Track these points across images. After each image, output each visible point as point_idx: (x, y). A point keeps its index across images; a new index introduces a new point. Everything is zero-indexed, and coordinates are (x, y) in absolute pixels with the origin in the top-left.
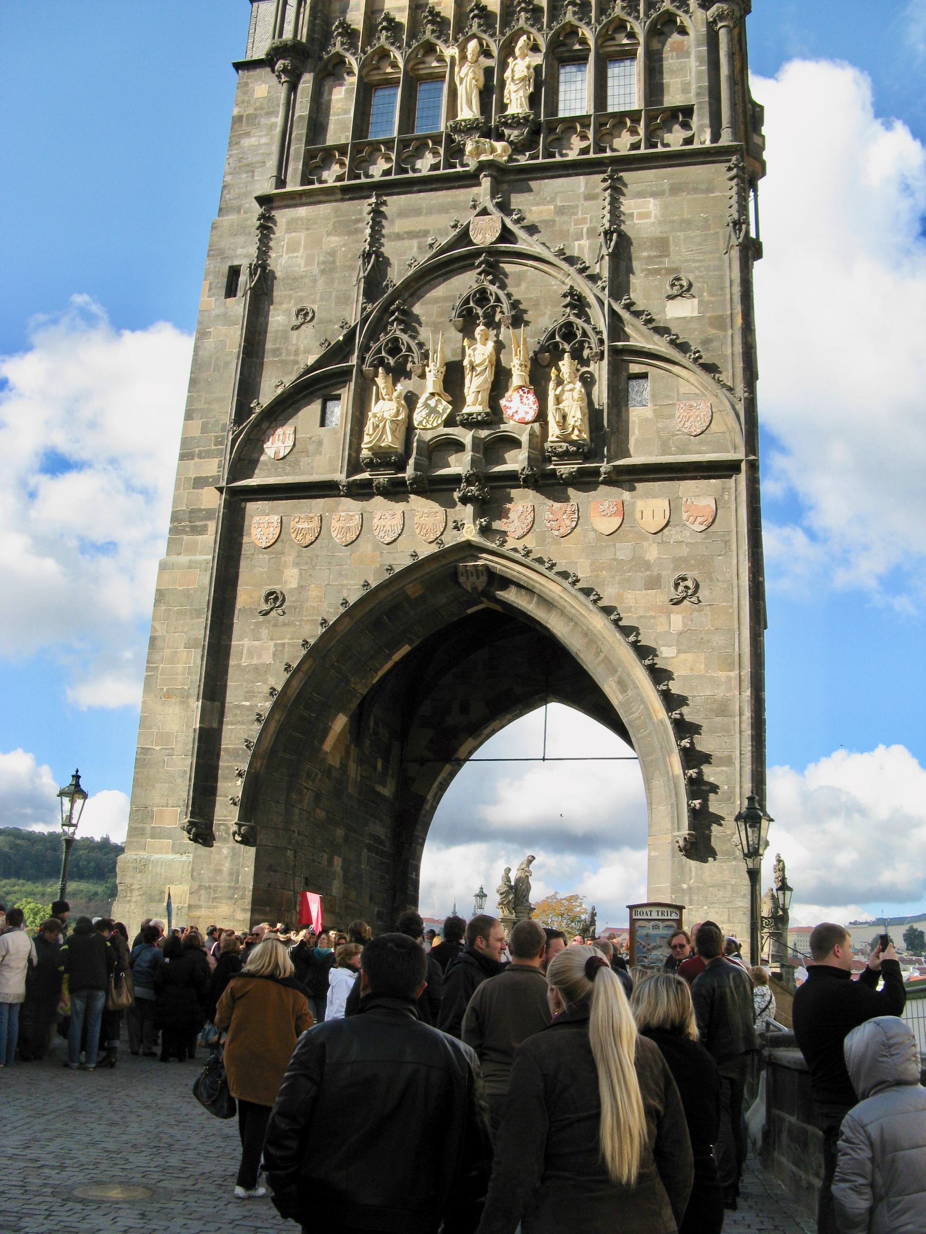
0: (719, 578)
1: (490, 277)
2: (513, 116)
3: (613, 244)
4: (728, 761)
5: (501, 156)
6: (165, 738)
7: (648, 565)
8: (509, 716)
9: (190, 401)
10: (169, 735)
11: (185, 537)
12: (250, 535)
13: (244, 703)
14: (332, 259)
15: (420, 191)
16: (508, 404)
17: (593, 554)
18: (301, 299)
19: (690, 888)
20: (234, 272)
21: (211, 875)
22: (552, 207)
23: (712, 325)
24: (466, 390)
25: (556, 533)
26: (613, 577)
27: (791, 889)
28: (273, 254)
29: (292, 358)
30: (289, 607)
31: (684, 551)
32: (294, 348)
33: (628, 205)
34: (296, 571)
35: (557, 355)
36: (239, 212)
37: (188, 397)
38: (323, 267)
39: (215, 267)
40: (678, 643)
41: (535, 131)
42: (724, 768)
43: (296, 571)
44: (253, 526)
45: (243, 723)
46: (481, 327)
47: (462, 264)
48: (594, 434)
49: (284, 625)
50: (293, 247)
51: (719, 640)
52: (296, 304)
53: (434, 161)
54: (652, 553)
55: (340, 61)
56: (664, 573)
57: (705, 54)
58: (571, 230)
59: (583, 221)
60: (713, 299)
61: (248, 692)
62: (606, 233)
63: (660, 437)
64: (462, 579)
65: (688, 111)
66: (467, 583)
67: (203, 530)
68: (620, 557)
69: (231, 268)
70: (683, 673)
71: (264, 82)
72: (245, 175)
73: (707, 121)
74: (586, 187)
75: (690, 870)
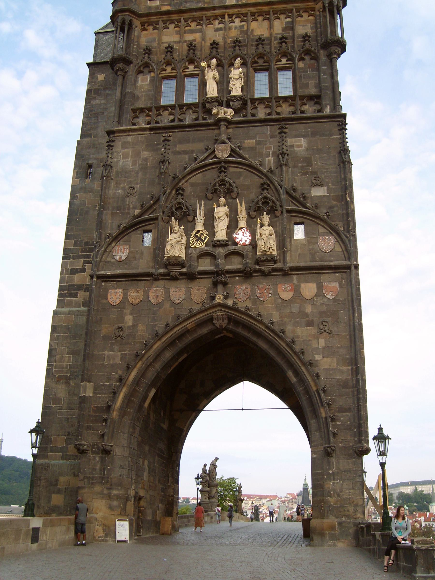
0: (342, 321)
2: (235, 96)
4: (349, 410)
6: (57, 401)
7: (307, 315)
8: (224, 388)
9: (67, 230)
10: (59, 399)
11: (66, 299)
12: (107, 299)
13: (106, 383)
14: (145, 163)
15: (189, 131)
16: (237, 236)
17: (280, 309)
18: (131, 182)
19: (333, 473)
21: (90, 471)
22: (254, 141)
23: (334, 200)
26: (290, 321)
29: (126, 211)
30: (127, 335)
31: (324, 308)
32: (127, 206)
33: (290, 141)
34: (131, 317)
36: (91, 137)
37: (67, 228)
38: (141, 166)
41: (245, 104)
42: (348, 414)
43: (131, 317)
44: (109, 294)
45: (105, 394)
46: (222, 198)
47: (211, 167)
48: (279, 251)
49: (126, 344)
50: (125, 156)
51: (343, 351)
52: (128, 185)
54: (309, 309)
55: (147, 65)
60: (334, 187)
61: (107, 378)
62: (281, 154)
63: (310, 253)
64: (215, 322)
67: (76, 295)
69: (88, 164)
70: (326, 367)
71: (103, 73)
74: (271, 131)
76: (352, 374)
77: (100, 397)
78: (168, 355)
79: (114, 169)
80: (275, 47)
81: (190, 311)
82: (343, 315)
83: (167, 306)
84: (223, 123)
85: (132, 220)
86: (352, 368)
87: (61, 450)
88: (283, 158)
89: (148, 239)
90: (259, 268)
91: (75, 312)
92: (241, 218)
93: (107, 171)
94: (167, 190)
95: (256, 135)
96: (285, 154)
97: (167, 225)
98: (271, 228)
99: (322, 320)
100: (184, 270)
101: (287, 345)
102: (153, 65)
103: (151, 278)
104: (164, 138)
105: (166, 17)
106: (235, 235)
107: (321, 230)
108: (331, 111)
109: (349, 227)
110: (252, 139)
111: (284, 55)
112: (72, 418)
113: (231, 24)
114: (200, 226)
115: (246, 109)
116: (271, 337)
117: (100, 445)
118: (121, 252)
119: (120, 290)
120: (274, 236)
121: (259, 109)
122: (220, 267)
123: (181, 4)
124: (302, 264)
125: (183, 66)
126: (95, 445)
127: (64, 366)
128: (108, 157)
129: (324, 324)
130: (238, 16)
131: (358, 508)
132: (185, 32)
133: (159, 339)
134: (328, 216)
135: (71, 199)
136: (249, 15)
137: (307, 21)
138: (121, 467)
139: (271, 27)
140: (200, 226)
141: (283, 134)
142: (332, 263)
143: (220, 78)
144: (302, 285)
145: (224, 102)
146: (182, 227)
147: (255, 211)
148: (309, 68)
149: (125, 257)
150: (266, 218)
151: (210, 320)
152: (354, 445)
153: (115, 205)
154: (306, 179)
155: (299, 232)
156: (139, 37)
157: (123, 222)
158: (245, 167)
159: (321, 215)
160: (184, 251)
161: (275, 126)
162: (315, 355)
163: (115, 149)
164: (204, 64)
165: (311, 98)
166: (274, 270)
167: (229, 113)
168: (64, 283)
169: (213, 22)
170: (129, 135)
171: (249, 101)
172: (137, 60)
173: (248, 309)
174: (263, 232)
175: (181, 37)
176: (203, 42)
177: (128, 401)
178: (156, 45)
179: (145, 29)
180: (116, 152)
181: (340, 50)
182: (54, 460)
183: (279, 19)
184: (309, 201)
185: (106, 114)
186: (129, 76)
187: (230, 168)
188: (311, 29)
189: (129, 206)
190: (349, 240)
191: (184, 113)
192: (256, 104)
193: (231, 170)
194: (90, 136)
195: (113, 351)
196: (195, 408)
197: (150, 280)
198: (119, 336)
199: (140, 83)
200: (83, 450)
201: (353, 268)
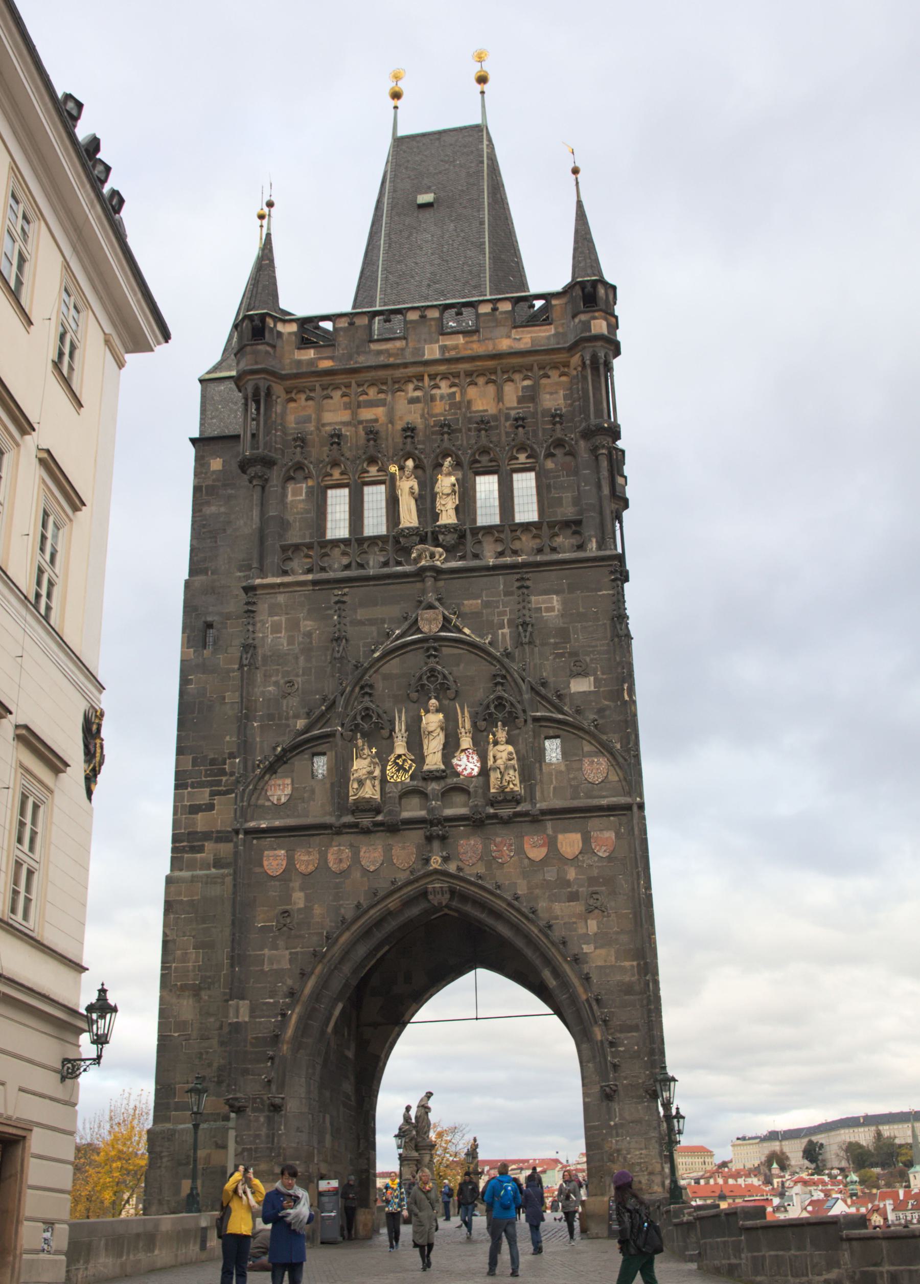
1: (437, 659)
2: (445, 526)
3: (528, 634)
4: (635, 1028)
6: (181, 1025)
7: (568, 883)
8: (444, 983)
10: (185, 1023)
11: (186, 855)
12: (262, 866)
15: (374, 585)
16: (459, 763)
19: (615, 1125)
23: (605, 699)
27: (683, 1118)
31: (595, 872)
35: (491, 721)
36: (207, 574)
41: (462, 536)
42: (634, 1034)
45: (268, 1017)
46: (433, 701)
47: (413, 647)
50: (276, 629)
51: (624, 938)
52: (283, 677)
53: (382, 559)
54: (571, 874)
55: (299, 467)
56: (581, 890)
58: (495, 621)
59: (504, 613)
60: (605, 677)
61: (271, 992)
62: (522, 625)
63: (571, 786)
64: (431, 897)
65: (578, 523)
66: (435, 900)
67: (201, 849)
69: (205, 622)
70: (599, 964)
72: (209, 541)
73: (593, 533)
76: (639, 973)
77: (260, 1023)
78: (362, 951)
79: (260, 651)
80: (507, 433)
81: (393, 883)
82: (623, 884)
83: (356, 875)
84: (428, 574)
85: (294, 739)
86: (638, 965)
88: (525, 631)
89: (321, 765)
92: (463, 734)
93: (249, 656)
94: (346, 687)
95: (482, 590)
96: (528, 624)
97: (349, 744)
98: (510, 748)
100: (380, 818)
101: (540, 931)
102: (311, 466)
103: (330, 831)
104: (337, 599)
105: (326, 380)
106: (455, 761)
107: (587, 748)
108: (599, 548)
109: (629, 743)
110: (477, 598)
111: (522, 448)
112: (207, 1053)
113: (434, 391)
114: (400, 748)
115: (464, 544)
117: (265, 1097)
118: (280, 790)
119: (283, 852)
120: (514, 762)
121: (485, 544)
122: (436, 812)
123: (350, 357)
124: (558, 803)
125: (360, 468)
127: (191, 968)
128: (248, 630)
129: (595, 896)
130: (445, 377)
131: (653, 1178)
132: (359, 406)
133: (348, 929)
134: (596, 726)
135: (181, 685)
136: (462, 373)
137: (557, 384)
138: (298, 1130)
139: (500, 397)
140: (400, 748)
141: (525, 591)
142: (604, 802)
143: (420, 490)
144: (560, 837)
145: (429, 534)
146: (374, 750)
147: (485, 720)
149: (287, 798)
151: (424, 894)
152: (644, 1082)
155: (553, 750)
156: (284, 414)
157: (280, 739)
159: (585, 724)
160: (378, 788)
161: (511, 576)
164: (393, 469)
165: (566, 524)
166: (517, 815)
167: (440, 558)
168: (180, 829)
169: (404, 388)
170: (280, 593)
171: (468, 532)
172: (283, 456)
173: (480, 877)
174: (499, 755)
175: (354, 414)
176: (390, 426)
177: (303, 1027)
178: (312, 429)
179: (292, 400)
180: (260, 621)
181: (610, 440)
183: (512, 381)
184: (567, 700)
185: (229, 531)
186: (273, 486)
187: (444, 649)
188: (564, 399)
189: (288, 713)
190: (629, 764)
191: (366, 552)
192: (480, 536)
193: (446, 651)
194: (204, 571)
195: (277, 949)
196: (396, 1019)
199: (290, 498)
200: (239, 1108)
201: (635, 808)
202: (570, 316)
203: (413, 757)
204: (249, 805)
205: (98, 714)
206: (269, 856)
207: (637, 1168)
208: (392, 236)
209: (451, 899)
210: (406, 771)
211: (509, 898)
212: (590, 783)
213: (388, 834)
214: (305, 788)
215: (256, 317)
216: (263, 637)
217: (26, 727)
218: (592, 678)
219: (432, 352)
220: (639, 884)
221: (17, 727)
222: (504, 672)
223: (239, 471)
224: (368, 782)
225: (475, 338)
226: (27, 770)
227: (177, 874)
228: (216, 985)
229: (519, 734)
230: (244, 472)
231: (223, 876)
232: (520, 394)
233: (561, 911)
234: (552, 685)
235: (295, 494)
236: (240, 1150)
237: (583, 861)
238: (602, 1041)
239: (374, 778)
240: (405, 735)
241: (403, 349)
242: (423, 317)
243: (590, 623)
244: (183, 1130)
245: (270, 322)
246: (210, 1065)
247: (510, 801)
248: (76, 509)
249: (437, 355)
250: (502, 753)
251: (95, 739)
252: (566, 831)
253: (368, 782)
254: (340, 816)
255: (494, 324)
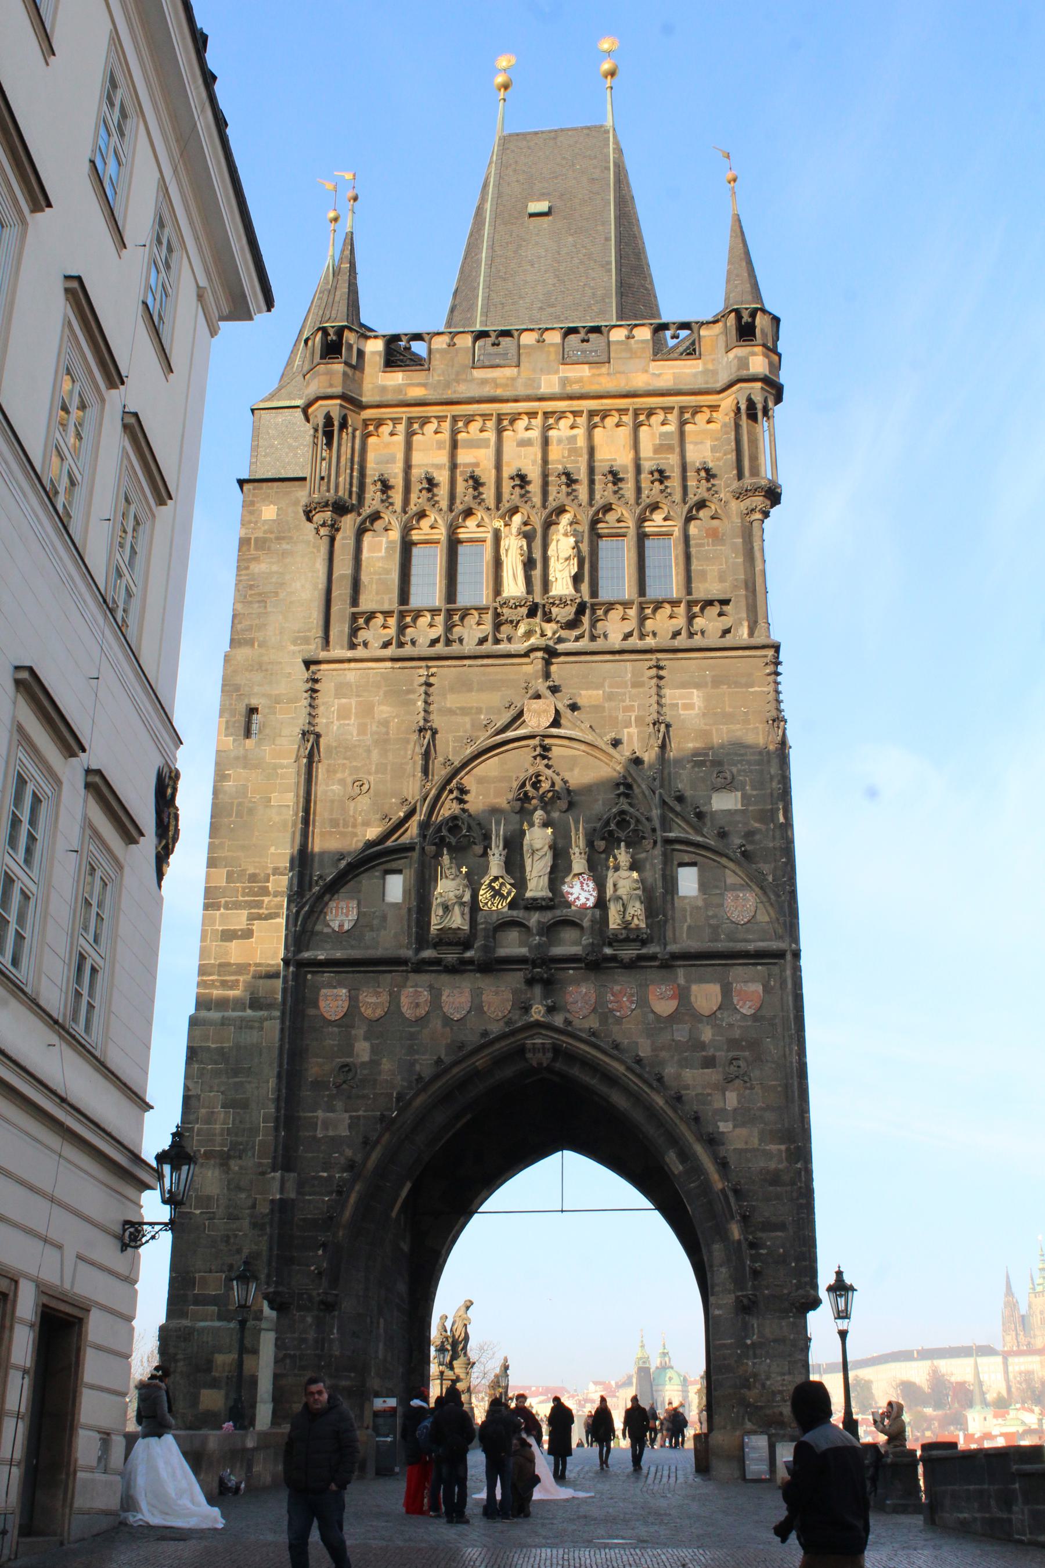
0: (769, 1058)
1: (546, 761)
4: (782, 1227)
5: (550, 639)
7: (702, 1046)
9: (212, 848)
10: (209, 1198)
12: (316, 1006)
13: (321, 1174)
14: (384, 730)
18: (356, 769)
19: (753, 1344)
20: (253, 711)
24: (528, 873)
25: (618, 1014)
28: (321, 721)
29: (350, 829)
31: (737, 1034)
35: (612, 841)
36: (253, 645)
38: (376, 737)
39: (231, 704)
40: (734, 1120)
42: (779, 1234)
44: (321, 998)
50: (344, 714)
51: (770, 1116)
52: (351, 774)
54: (707, 1034)
56: (718, 1054)
57: (741, 546)
60: (755, 793)
62: (654, 724)
63: (710, 926)
64: (529, 1055)
65: (725, 602)
66: (534, 1059)
68: (678, 1037)
70: (740, 1145)
71: (271, 503)
72: (257, 605)
73: (744, 615)
74: (633, 675)
75: (753, 1325)
83: (437, 1024)
86: (788, 1150)
87: (214, 1300)
89: (395, 888)
90: (614, 955)
91: (234, 1019)
94: (431, 789)
95: (604, 679)
97: (433, 861)
98: (635, 875)
99: (731, 1054)
100: (469, 954)
105: (416, 411)
106: (565, 888)
107: (731, 879)
108: (751, 634)
110: (597, 688)
112: (236, 1236)
116: (636, 1088)
117: (314, 1293)
119: (344, 991)
120: (639, 892)
123: (447, 385)
126: (302, 1294)
127: (217, 1131)
133: (424, 1089)
134: (744, 854)
137: (705, 432)
142: (751, 947)
144: (694, 988)
146: (464, 870)
147: (603, 839)
148: (707, 536)
150: (623, 856)
151: (521, 1051)
152: (790, 1293)
153: (326, 815)
154: (702, 775)
158: (583, 747)
160: (467, 917)
162: (719, 1123)
163: (321, 699)
165: (710, 603)
166: (641, 958)
168: (210, 959)
173: (594, 1034)
174: (621, 883)
178: (396, 471)
180: (323, 704)
182: (202, 1320)
185: (282, 595)
189: (356, 820)
194: (250, 643)
195: (333, 1111)
197: (403, 971)
198: (344, 1082)
199: (365, 554)
201: (789, 957)
202: (723, 350)
203: (512, 881)
204: (304, 930)
205: (173, 775)
206: (326, 996)
207: (778, 1398)
208: (497, 248)
209: (554, 1059)
210: (504, 898)
211: (629, 1061)
212: (733, 922)
213: (478, 975)
214: (374, 913)
215: (331, 331)
216: (327, 725)
217: (99, 772)
218: (739, 794)
219: (549, 384)
220: (791, 1050)
221: (88, 771)
222: (630, 780)
223: (304, 518)
224: (456, 908)
225: (604, 369)
226: (96, 834)
227: (204, 1014)
228: (250, 1154)
229: (646, 859)
230: (309, 519)
231: (262, 1020)
232: (658, 442)
233: (694, 1079)
234: (689, 800)
235: (371, 550)
236: (281, 1355)
237: (722, 1020)
238: (739, 1242)
239: (463, 904)
240: (504, 853)
241: (513, 379)
242: (540, 341)
243: (738, 726)
244: (203, 1329)
245: (349, 337)
246: (239, 1251)
247: (634, 940)
248: (161, 502)
249: (556, 389)
250: (624, 881)
251: (169, 807)
252: (701, 980)
253: (456, 908)
254: (418, 950)
255: (628, 355)
